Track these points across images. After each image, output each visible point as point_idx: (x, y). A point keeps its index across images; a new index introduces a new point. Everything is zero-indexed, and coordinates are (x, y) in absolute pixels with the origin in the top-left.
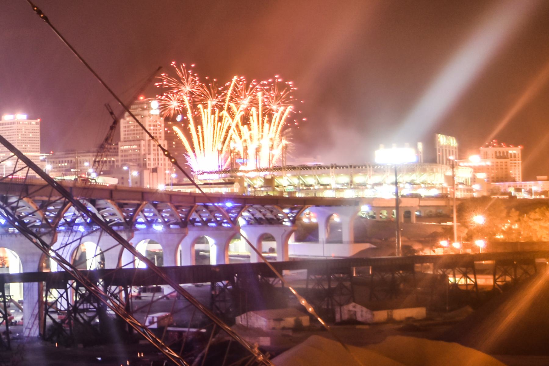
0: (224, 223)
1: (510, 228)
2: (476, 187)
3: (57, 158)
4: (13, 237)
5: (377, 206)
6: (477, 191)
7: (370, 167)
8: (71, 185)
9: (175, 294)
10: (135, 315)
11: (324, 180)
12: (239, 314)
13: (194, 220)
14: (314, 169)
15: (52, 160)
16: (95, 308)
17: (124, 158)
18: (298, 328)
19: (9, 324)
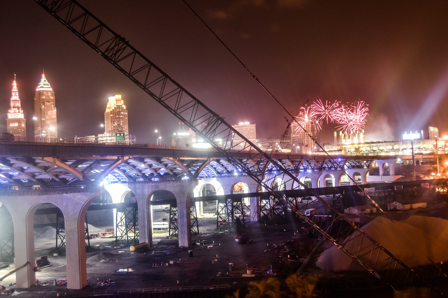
0: (338, 168)
3: (263, 141)
4: (245, 177)
5: (404, 159)
7: (401, 142)
8: (270, 153)
9: (317, 200)
10: (300, 210)
11: (381, 148)
14: (377, 143)
15: (261, 142)
16: (282, 207)
17: (293, 141)
18: (371, 213)
19: (244, 216)
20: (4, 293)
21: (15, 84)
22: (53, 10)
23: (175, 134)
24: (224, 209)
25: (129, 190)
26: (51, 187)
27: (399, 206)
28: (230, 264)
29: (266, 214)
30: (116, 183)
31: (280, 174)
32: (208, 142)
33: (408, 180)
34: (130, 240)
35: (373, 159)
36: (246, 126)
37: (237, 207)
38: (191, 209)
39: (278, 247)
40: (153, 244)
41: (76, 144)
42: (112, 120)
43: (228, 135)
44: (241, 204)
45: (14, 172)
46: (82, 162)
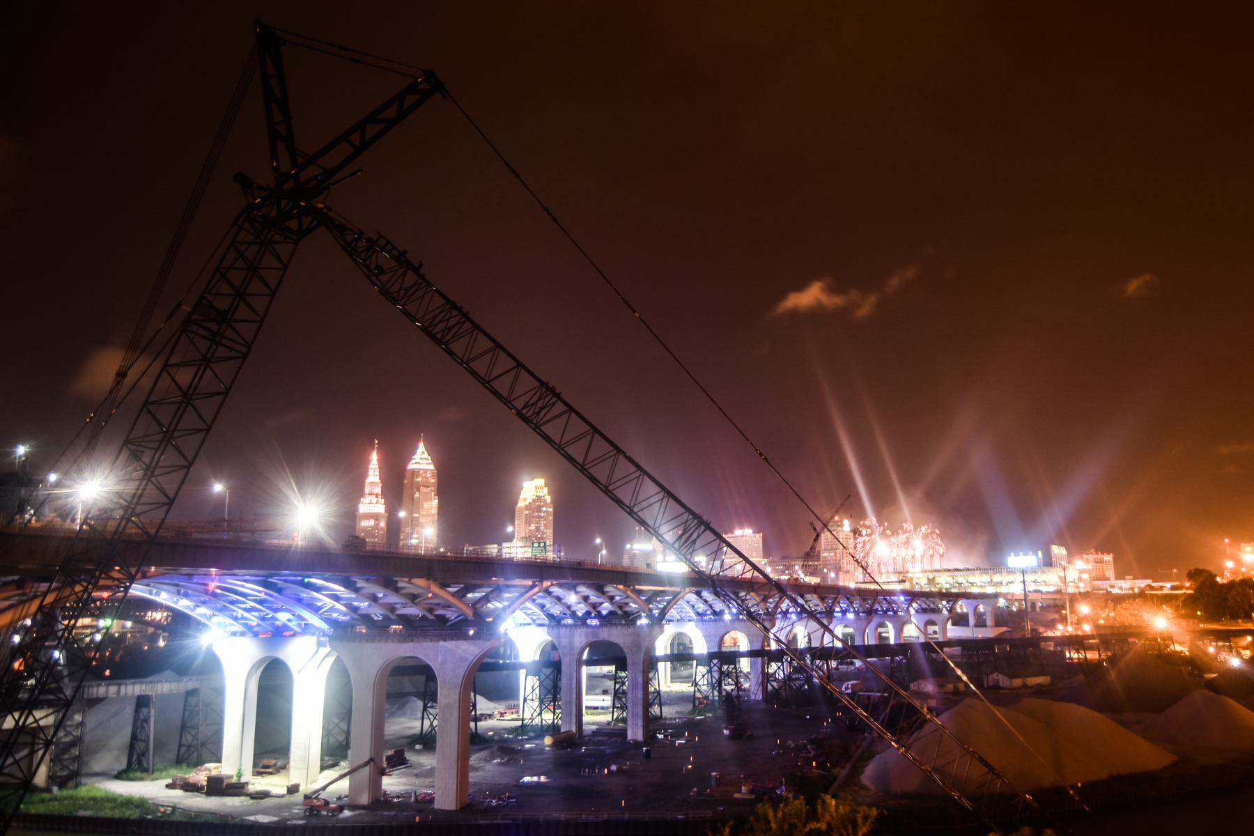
1: (1108, 615)
2: (1082, 585)
4: (743, 623)
6: (1083, 588)
8: (786, 583)
9: (864, 666)
11: (972, 579)
12: (913, 682)
13: (877, 609)
17: (824, 563)
18: (956, 692)
20: (326, 813)
21: (374, 457)
22: (444, 340)
23: (628, 546)
24: (706, 676)
25: (549, 638)
26: (421, 630)
27: (1003, 680)
28: (714, 774)
29: (776, 687)
30: (528, 626)
31: (802, 618)
32: (682, 561)
33: (1017, 636)
34: (546, 725)
35: (958, 598)
36: (746, 536)
37: (728, 675)
38: (651, 675)
39: (796, 746)
40: (584, 733)
41: (466, 557)
42: (526, 520)
43: (717, 551)
44: (735, 668)
45: (361, 602)
46: (472, 588)
